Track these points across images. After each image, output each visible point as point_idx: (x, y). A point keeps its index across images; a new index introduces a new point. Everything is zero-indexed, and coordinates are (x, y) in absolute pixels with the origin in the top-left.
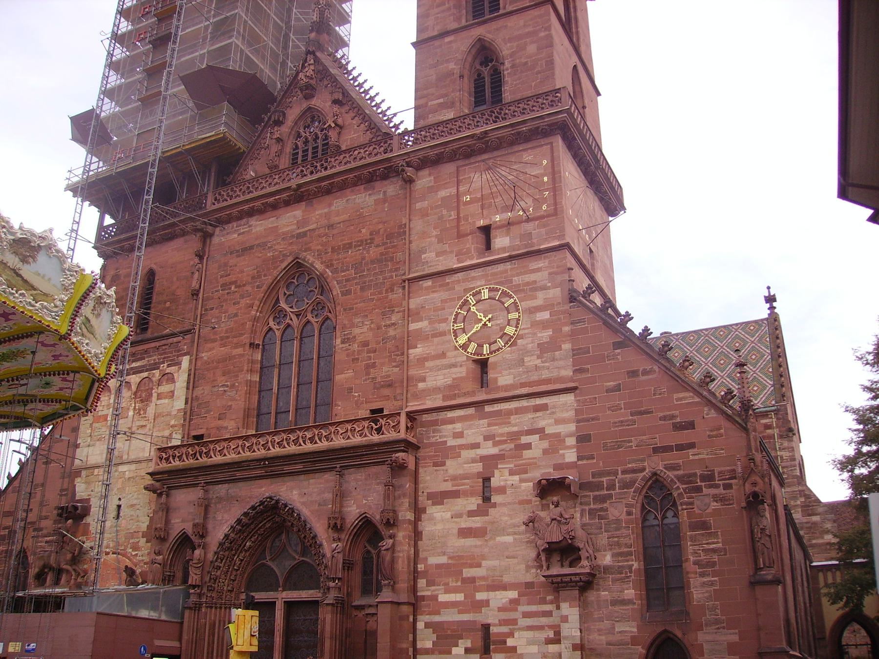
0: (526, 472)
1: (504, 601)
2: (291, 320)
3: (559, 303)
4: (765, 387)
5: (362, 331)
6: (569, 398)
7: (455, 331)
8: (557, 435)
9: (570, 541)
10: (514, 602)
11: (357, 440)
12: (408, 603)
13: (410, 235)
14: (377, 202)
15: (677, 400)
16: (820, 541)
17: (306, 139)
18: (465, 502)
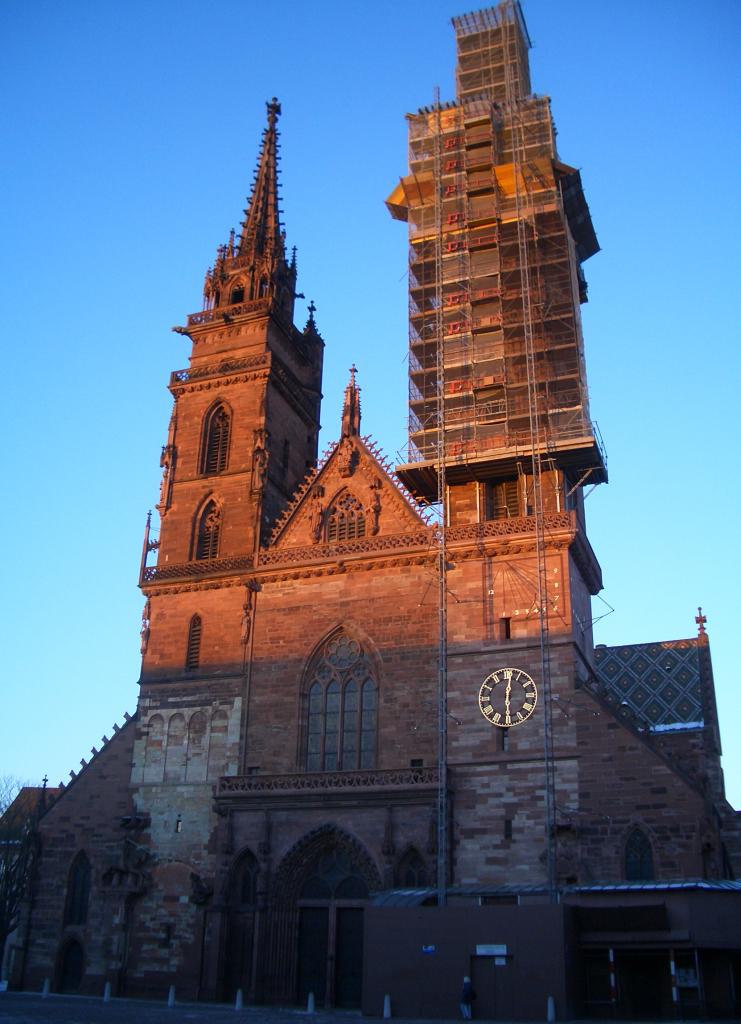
0: (539, 817)
6: (573, 763)
7: (483, 703)
11: (405, 786)
14: (413, 584)
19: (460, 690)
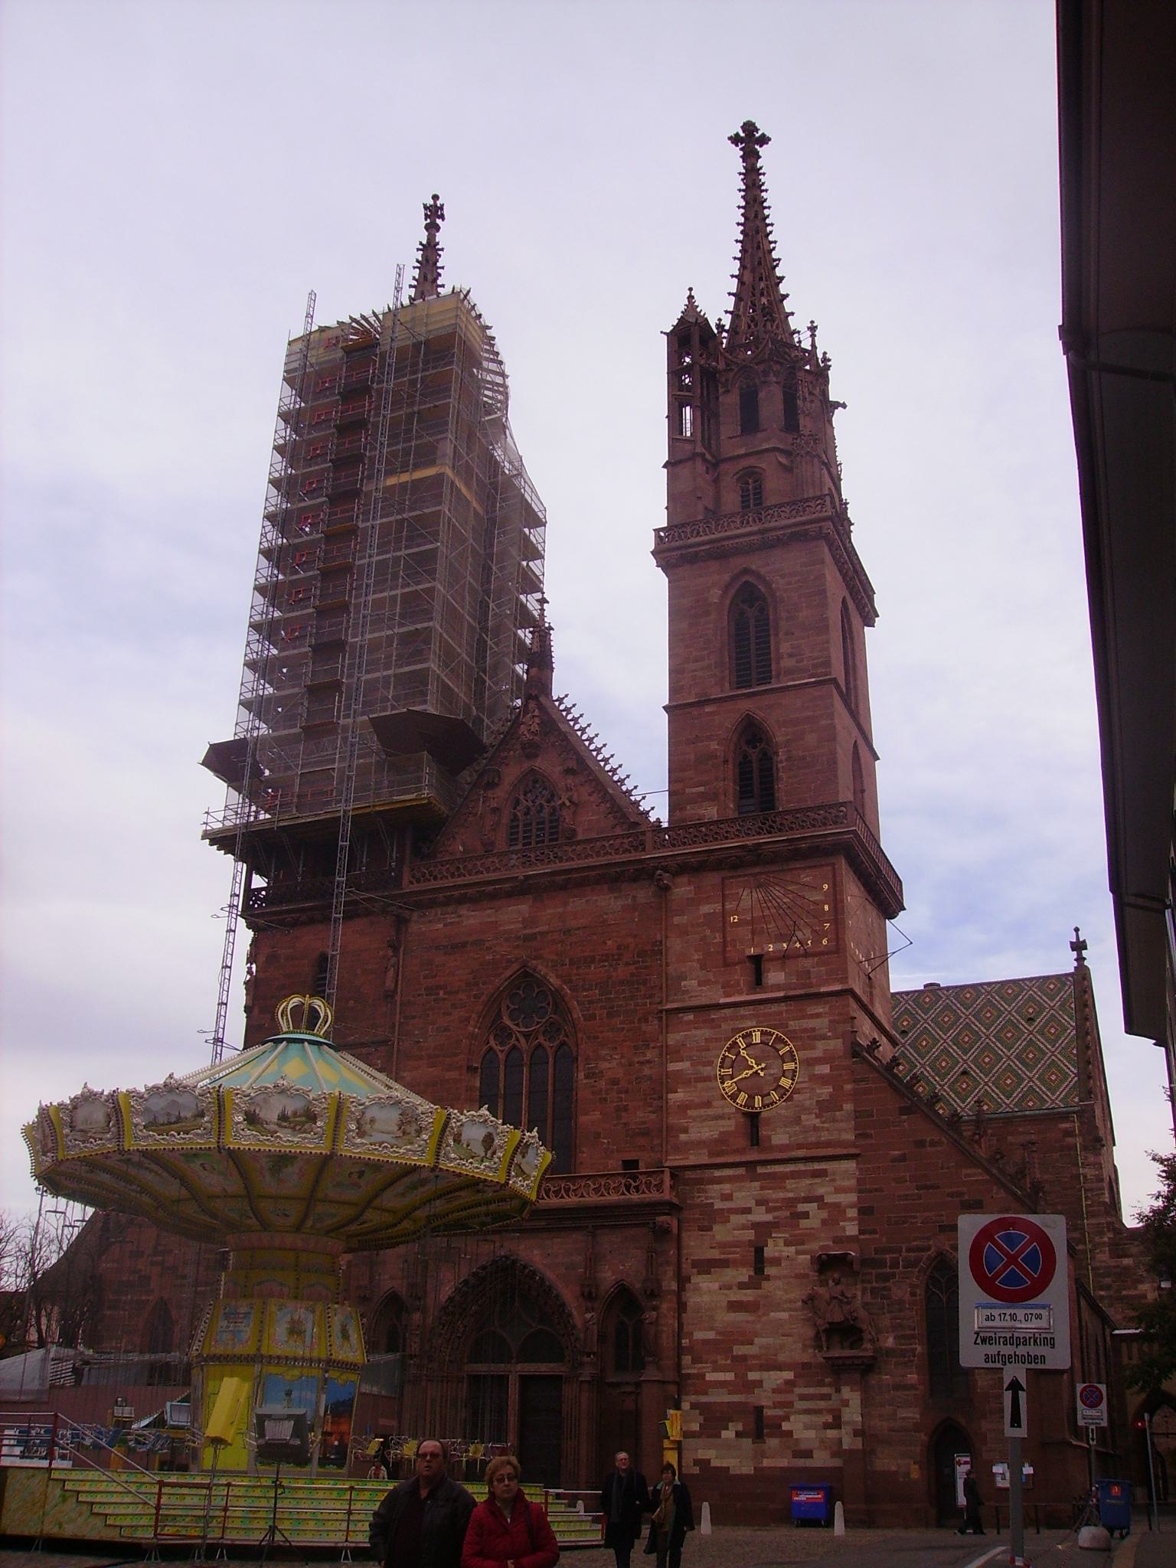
1: (778, 1382)
2: (518, 1040)
3: (840, 1057)
4: (1066, 1076)
5: (611, 1065)
6: (850, 1165)
8: (837, 1205)
9: (852, 1322)
10: (790, 1384)
11: (614, 1198)
12: (675, 1383)
13: (666, 954)
15: (967, 1175)
16: (1132, 1292)
17: (528, 808)
18: (735, 1272)
19: (690, 1058)
